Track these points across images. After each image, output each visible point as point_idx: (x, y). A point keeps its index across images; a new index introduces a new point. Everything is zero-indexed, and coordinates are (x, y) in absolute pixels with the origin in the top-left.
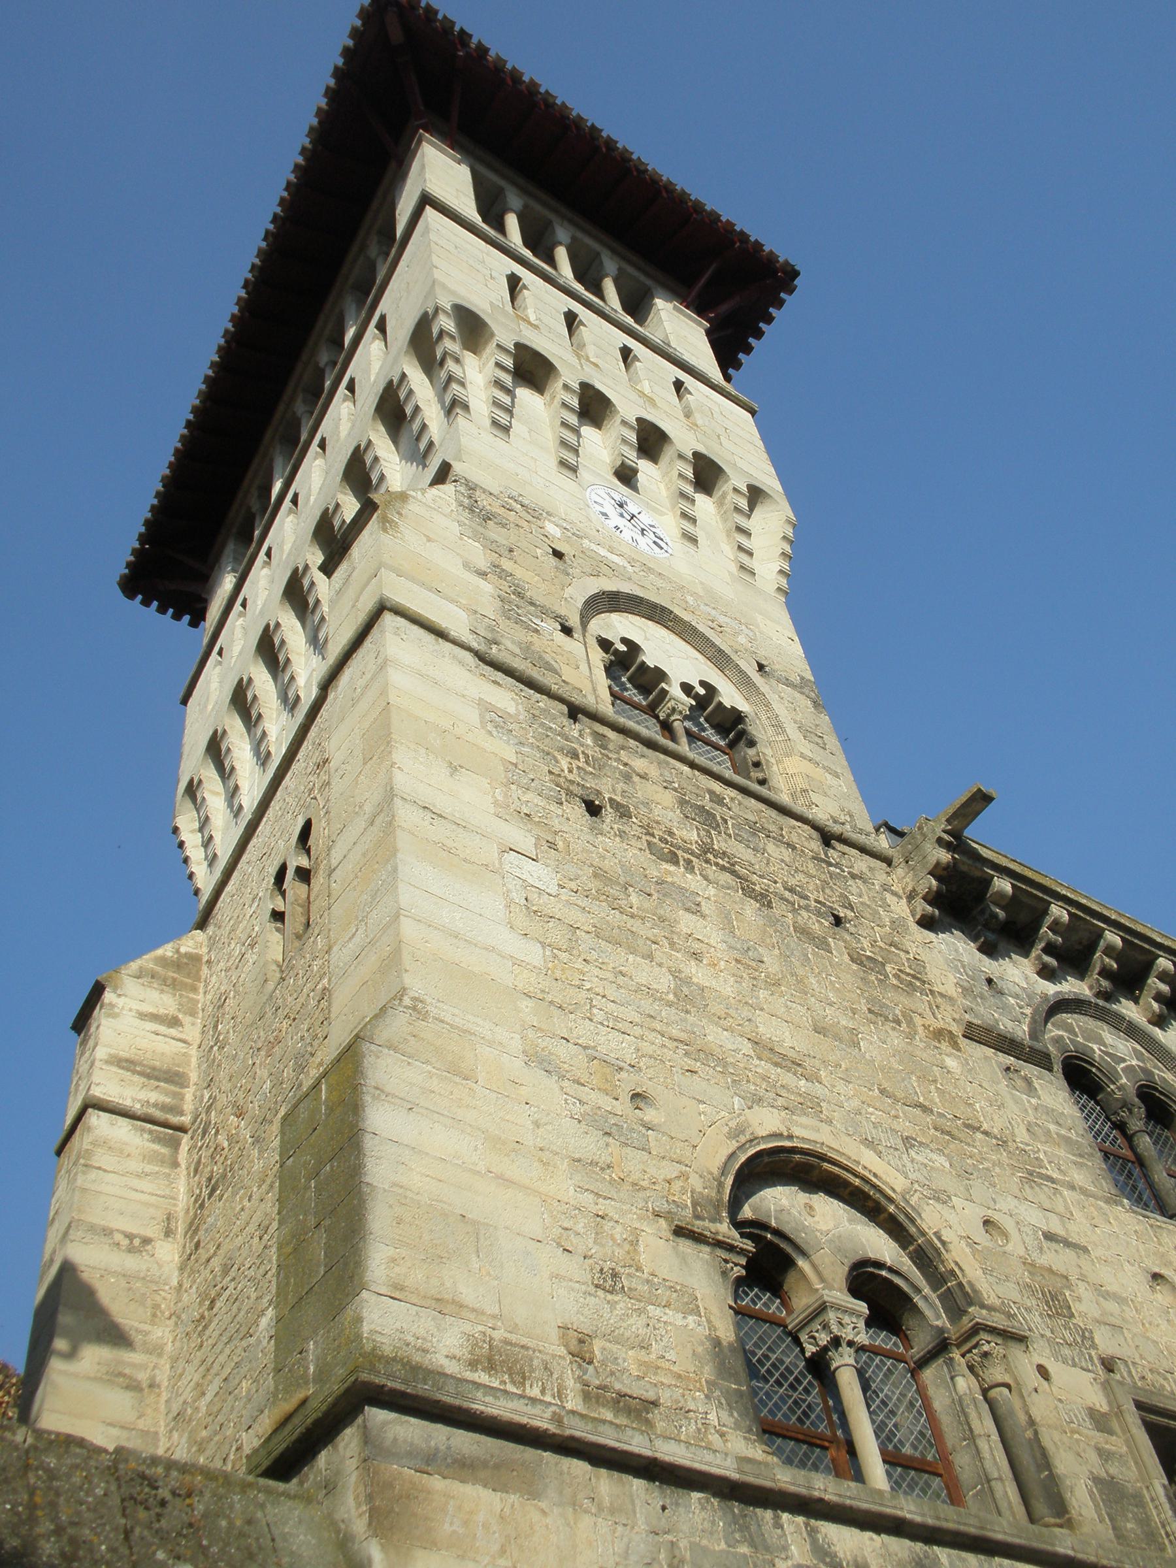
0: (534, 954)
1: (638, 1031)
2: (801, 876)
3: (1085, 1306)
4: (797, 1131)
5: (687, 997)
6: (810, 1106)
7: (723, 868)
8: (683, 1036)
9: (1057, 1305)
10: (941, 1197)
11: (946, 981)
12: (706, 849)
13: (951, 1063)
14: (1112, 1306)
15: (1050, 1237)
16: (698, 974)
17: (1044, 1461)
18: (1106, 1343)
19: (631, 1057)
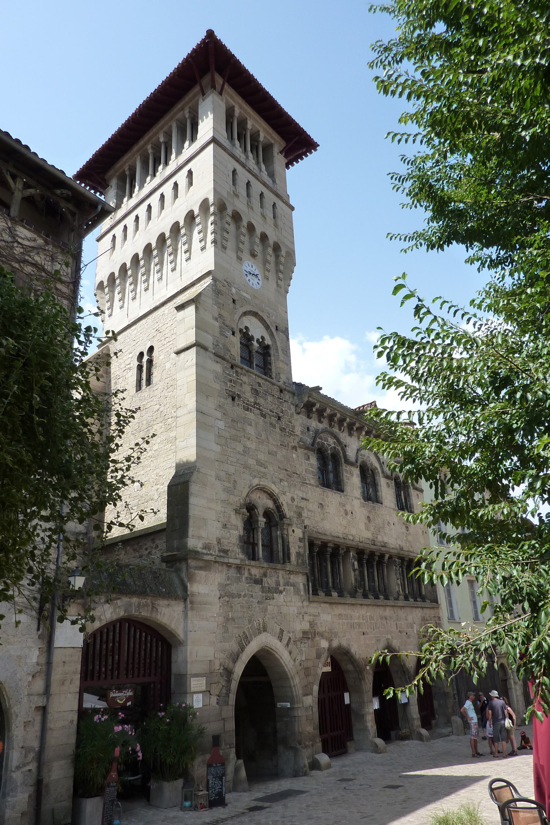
0: (218, 449)
1: (235, 464)
2: (274, 406)
3: (305, 514)
4: (261, 483)
5: (246, 451)
6: (264, 476)
7: (258, 409)
8: (243, 463)
9: (300, 515)
10: (284, 493)
11: (298, 430)
12: (255, 403)
13: (294, 455)
14: (310, 513)
15: (302, 499)
16: (248, 444)
17: (289, 549)
18: (306, 523)
19: (233, 471)
